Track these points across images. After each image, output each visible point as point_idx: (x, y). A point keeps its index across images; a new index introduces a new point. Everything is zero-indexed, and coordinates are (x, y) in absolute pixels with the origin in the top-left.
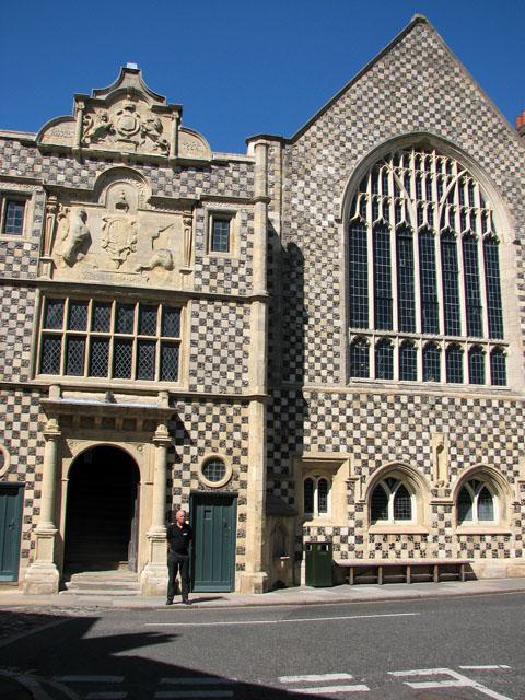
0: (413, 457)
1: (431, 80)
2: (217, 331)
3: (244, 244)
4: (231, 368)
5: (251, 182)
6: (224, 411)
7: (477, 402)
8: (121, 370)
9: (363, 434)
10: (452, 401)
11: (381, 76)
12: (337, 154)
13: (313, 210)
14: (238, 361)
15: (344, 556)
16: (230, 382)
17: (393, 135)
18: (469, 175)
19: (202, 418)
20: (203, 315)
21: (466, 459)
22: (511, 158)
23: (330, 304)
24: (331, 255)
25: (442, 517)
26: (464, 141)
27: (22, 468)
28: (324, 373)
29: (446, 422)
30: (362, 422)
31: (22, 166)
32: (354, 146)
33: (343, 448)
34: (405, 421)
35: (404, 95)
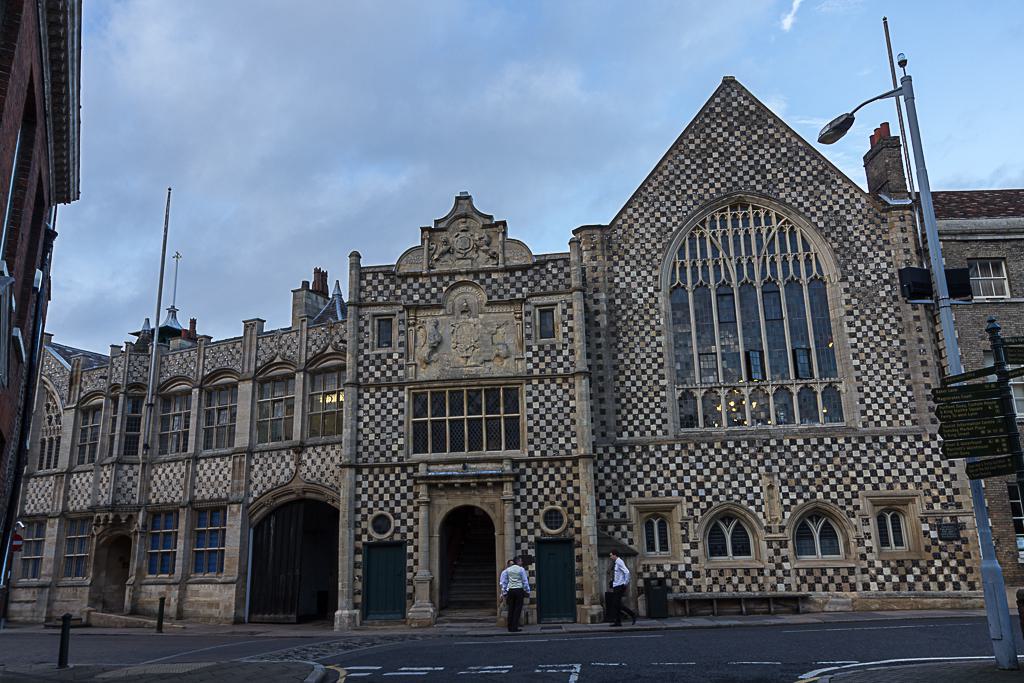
0: (744, 497)
1: (744, 138)
2: (548, 405)
3: (566, 330)
4: (561, 434)
5: (568, 275)
6: (558, 471)
7: (807, 441)
8: (475, 445)
9: (693, 479)
10: (780, 443)
11: (692, 147)
12: (653, 230)
13: (634, 285)
14: (567, 428)
15: (683, 589)
16: (562, 446)
17: (706, 200)
18: (789, 223)
19: (541, 478)
20: (535, 393)
21: (799, 496)
22: (835, 197)
23: (655, 366)
24: (653, 323)
25: (777, 552)
26: (781, 190)
27: (403, 529)
28: (653, 427)
29: (775, 462)
30: (691, 468)
31: (386, 293)
32: (669, 220)
33: (675, 493)
34: (733, 464)
35: (716, 160)
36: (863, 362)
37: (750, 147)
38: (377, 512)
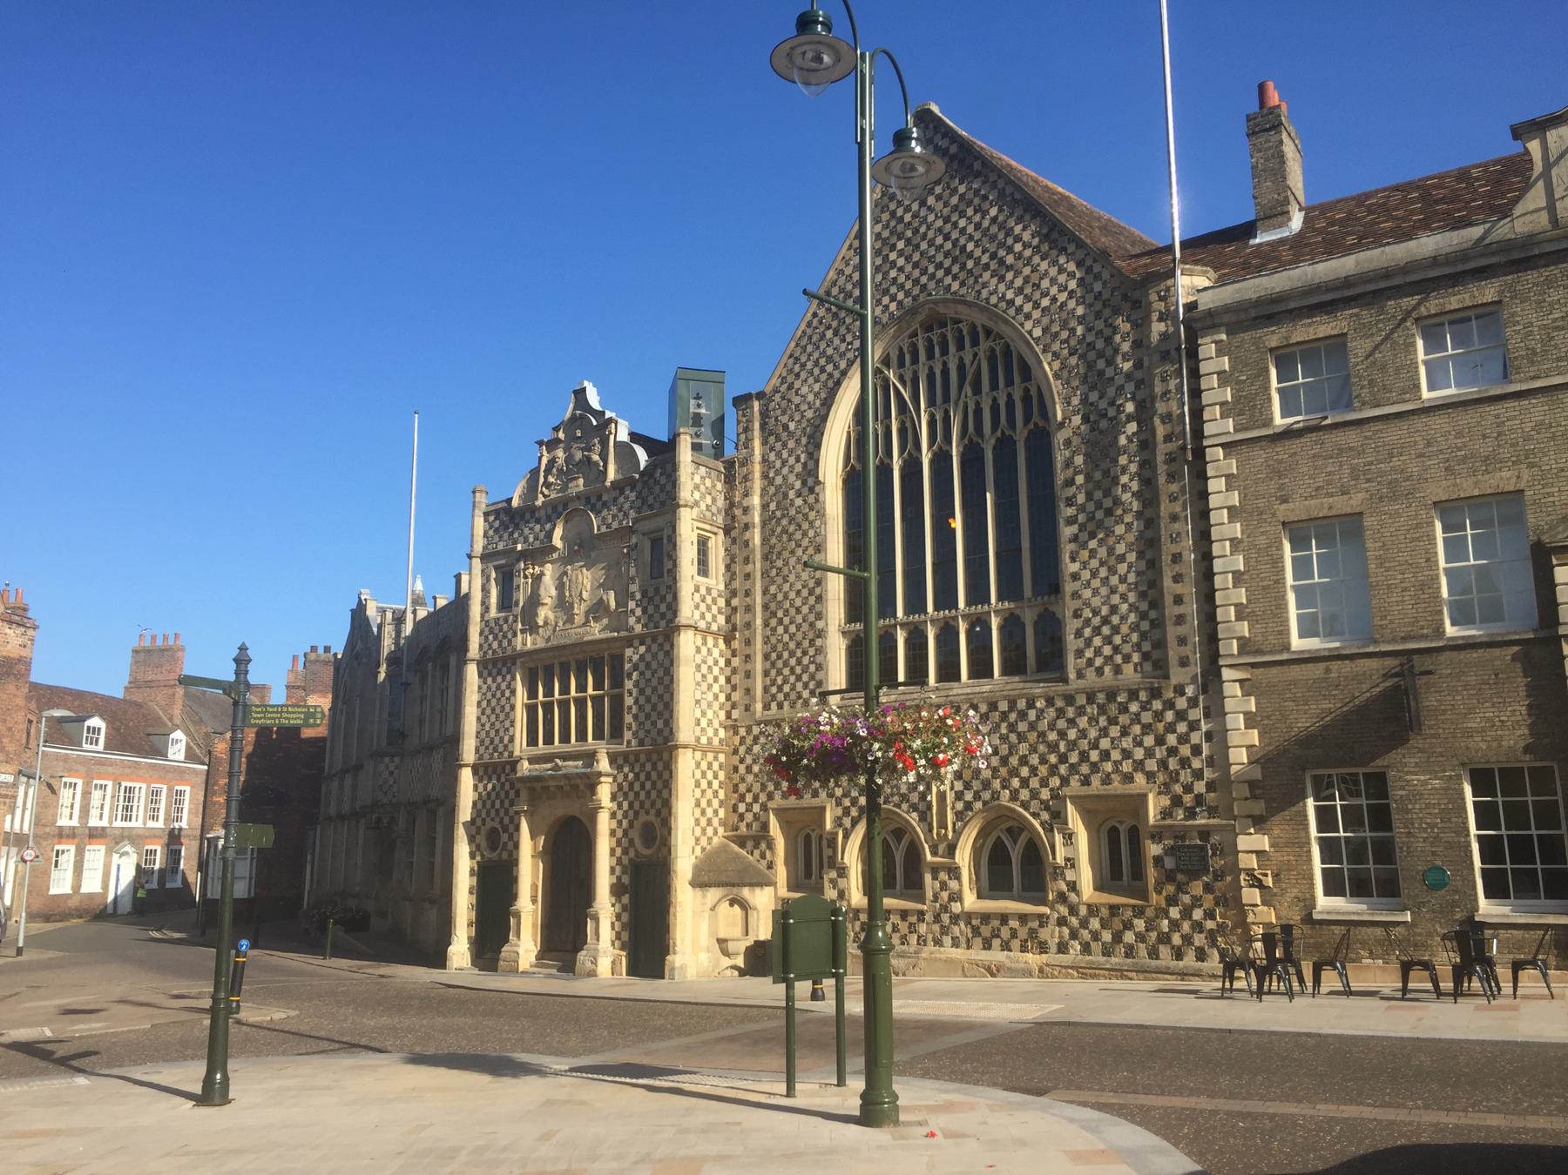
21: (977, 797)
26: (985, 285)
36: (1085, 565)
37: (947, 220)
38: (490, 824)
